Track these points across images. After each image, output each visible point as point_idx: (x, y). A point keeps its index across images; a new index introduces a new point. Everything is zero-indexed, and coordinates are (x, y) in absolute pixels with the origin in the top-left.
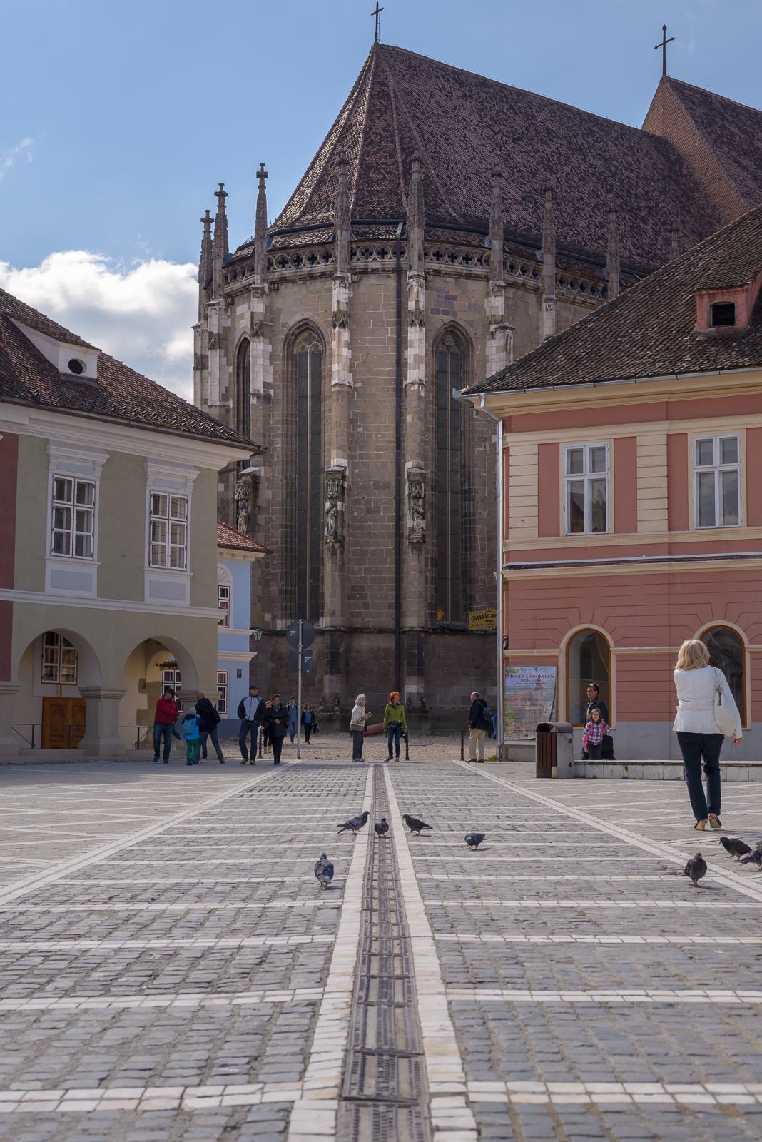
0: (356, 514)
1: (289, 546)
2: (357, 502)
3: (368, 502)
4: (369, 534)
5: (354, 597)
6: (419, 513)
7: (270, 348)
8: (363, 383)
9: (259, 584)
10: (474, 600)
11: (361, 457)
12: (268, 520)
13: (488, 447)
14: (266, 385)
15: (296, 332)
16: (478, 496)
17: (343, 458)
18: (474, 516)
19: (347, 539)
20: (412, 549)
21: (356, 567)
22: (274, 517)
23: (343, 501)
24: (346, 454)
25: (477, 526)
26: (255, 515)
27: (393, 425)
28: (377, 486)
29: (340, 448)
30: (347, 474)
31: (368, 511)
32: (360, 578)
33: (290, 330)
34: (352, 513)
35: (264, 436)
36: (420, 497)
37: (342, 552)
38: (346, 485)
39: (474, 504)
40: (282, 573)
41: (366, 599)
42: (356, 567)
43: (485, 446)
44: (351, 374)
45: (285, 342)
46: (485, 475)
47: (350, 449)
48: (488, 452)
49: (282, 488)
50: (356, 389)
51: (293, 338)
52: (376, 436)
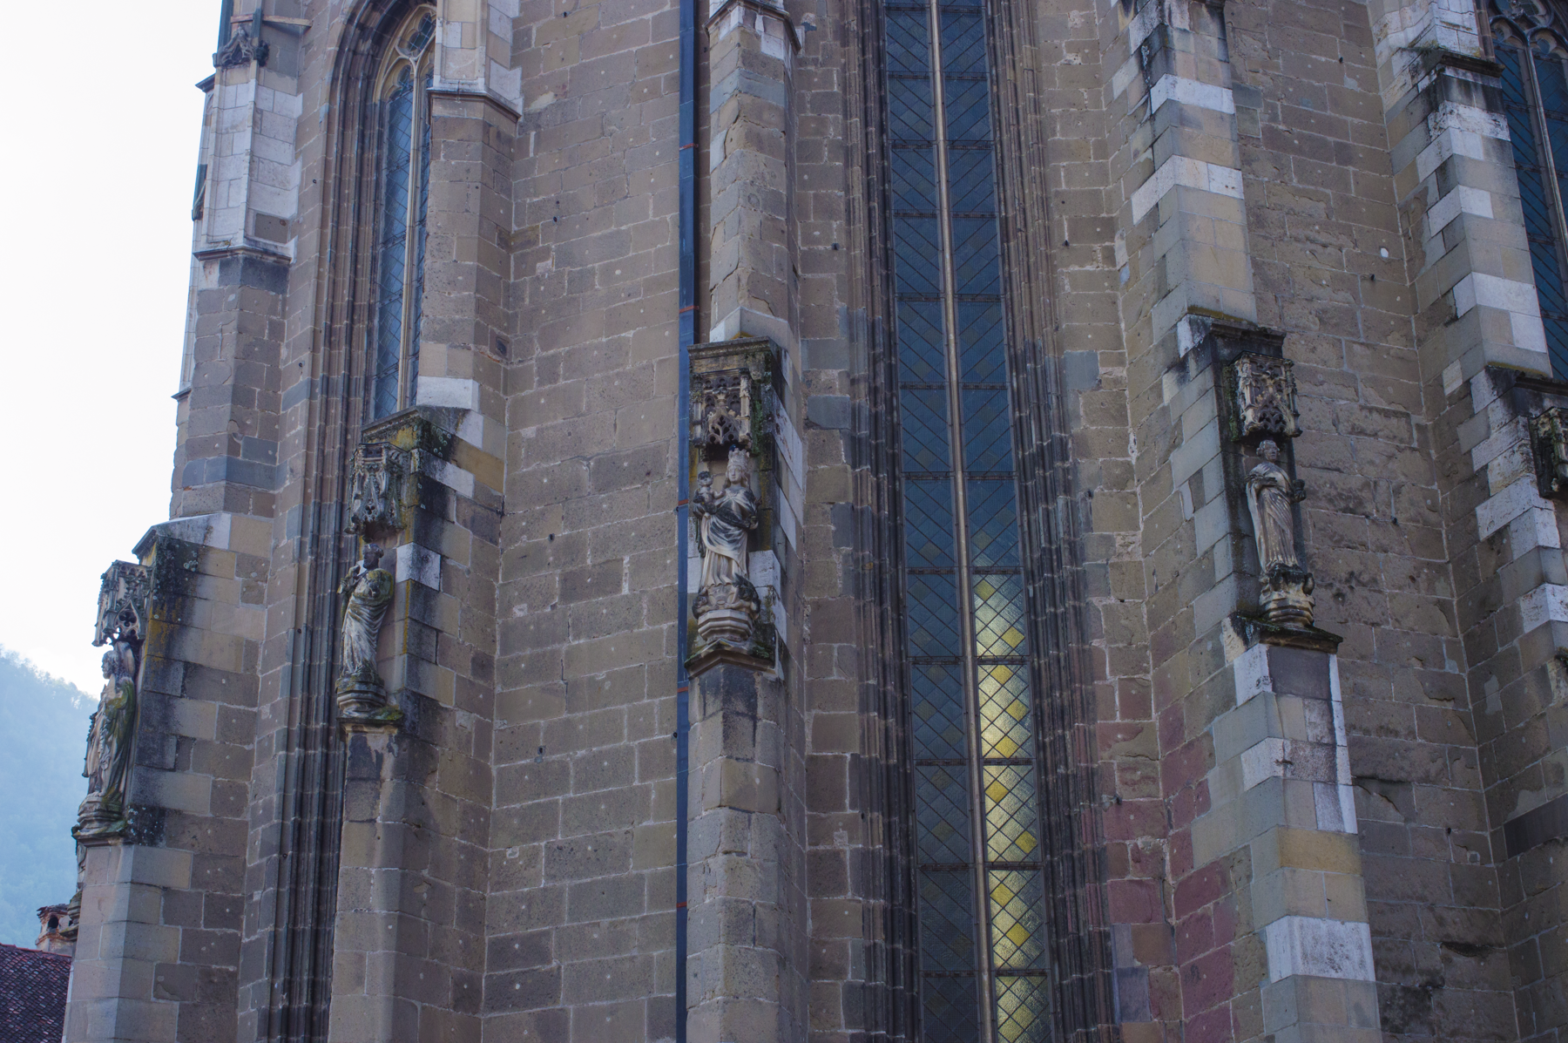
0: (519, 611)
1: (313, 819)
2: (529, 559)
3: (572, 549)
4: (571, 689)
5: (501, 997)
6: (724, 513)
7: (295, 105)
8: (562, 91)
9: (166, 989)
10: (1107, 958)
11: (549, 372)
12: (240, 727)
13: (1122, 256)
14: (263, 224)
15: (377, 18)
16: (1088, 468)
17: (452, 373)
18: (1076, 554)
19: (463, 719)
20: (703, 692)
21: (514, 853)
22: (265, 711)
23: (426, 540)
24: (466, 359)
25: (1097, 601)
26: (166, 702)
27: (671, 216)
28: (609, 474)
29: (444, 335)
30: (472, 433)
31: (572, 588)
32: (530, 899)
33: (350, 21)
34: (507, 610)
35: (240, 396)
36: (733, 443)
37: (415, 769)
38: (459, 480)
39: (1072, 508)
40: (275, 936)
41: (552, 995)
42: (514, 853)
43: (1110, 256)
44: (518, 72)
45: (337, 64)
46: (1121, 372)
47: (502, 347)
48: (1125, 276)
49: (299, 592)
50: (534, 119)
51: (365, 47)
52: (607, 272)
